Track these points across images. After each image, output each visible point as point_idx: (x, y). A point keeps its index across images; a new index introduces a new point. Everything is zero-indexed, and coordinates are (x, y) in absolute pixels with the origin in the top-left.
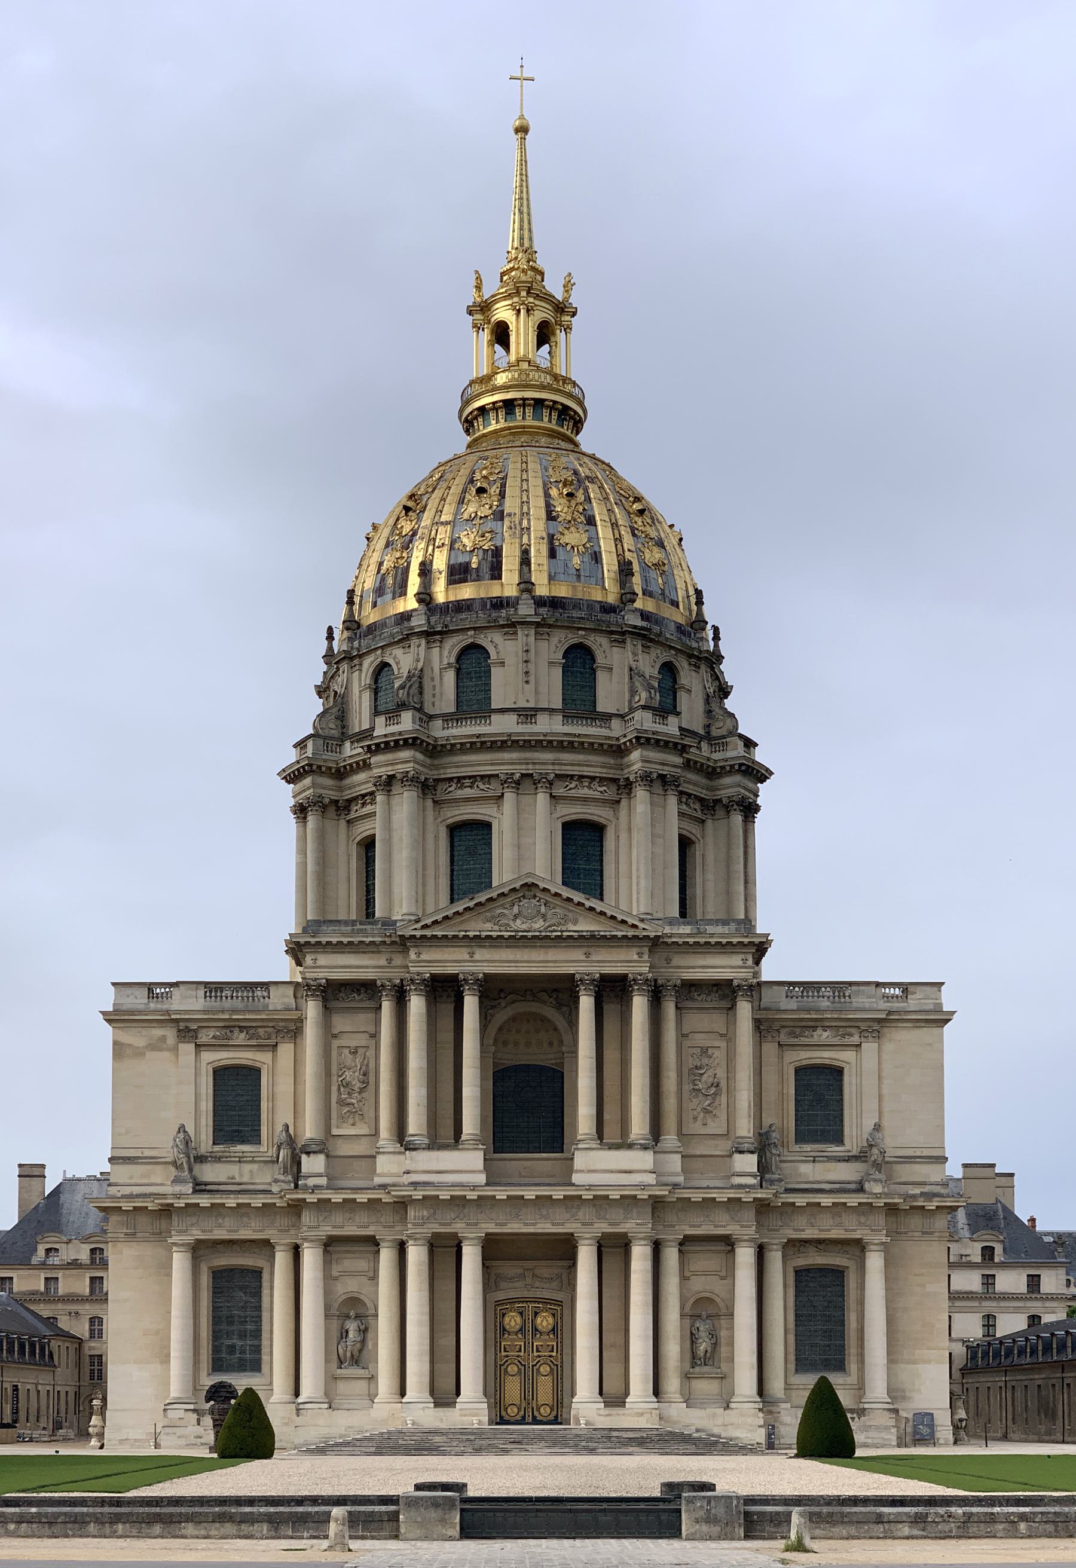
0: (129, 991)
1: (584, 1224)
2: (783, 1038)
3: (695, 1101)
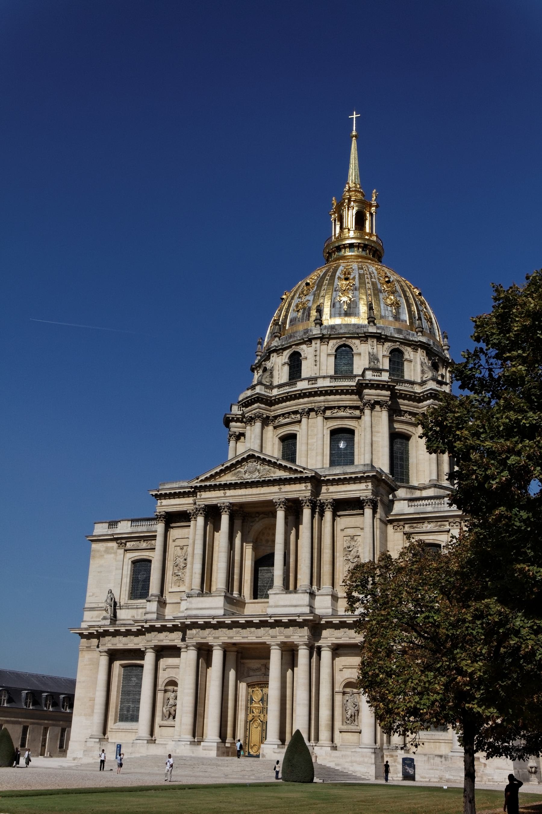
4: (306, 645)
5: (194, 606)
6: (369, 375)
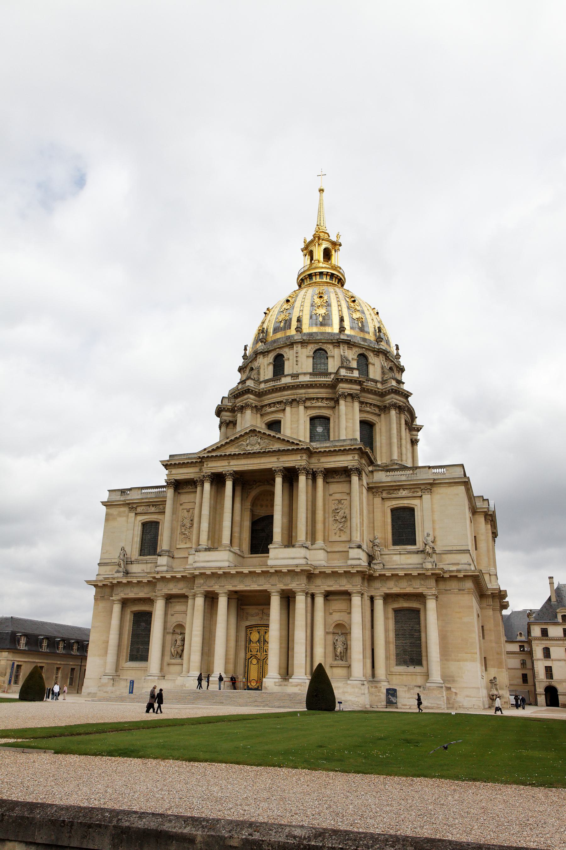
0: (114, 493)
1: (272, 585)
2: (385, 495)
3: (336, 525)
4: (303, 591)
5: (202, 559)
6: (343, 372)
